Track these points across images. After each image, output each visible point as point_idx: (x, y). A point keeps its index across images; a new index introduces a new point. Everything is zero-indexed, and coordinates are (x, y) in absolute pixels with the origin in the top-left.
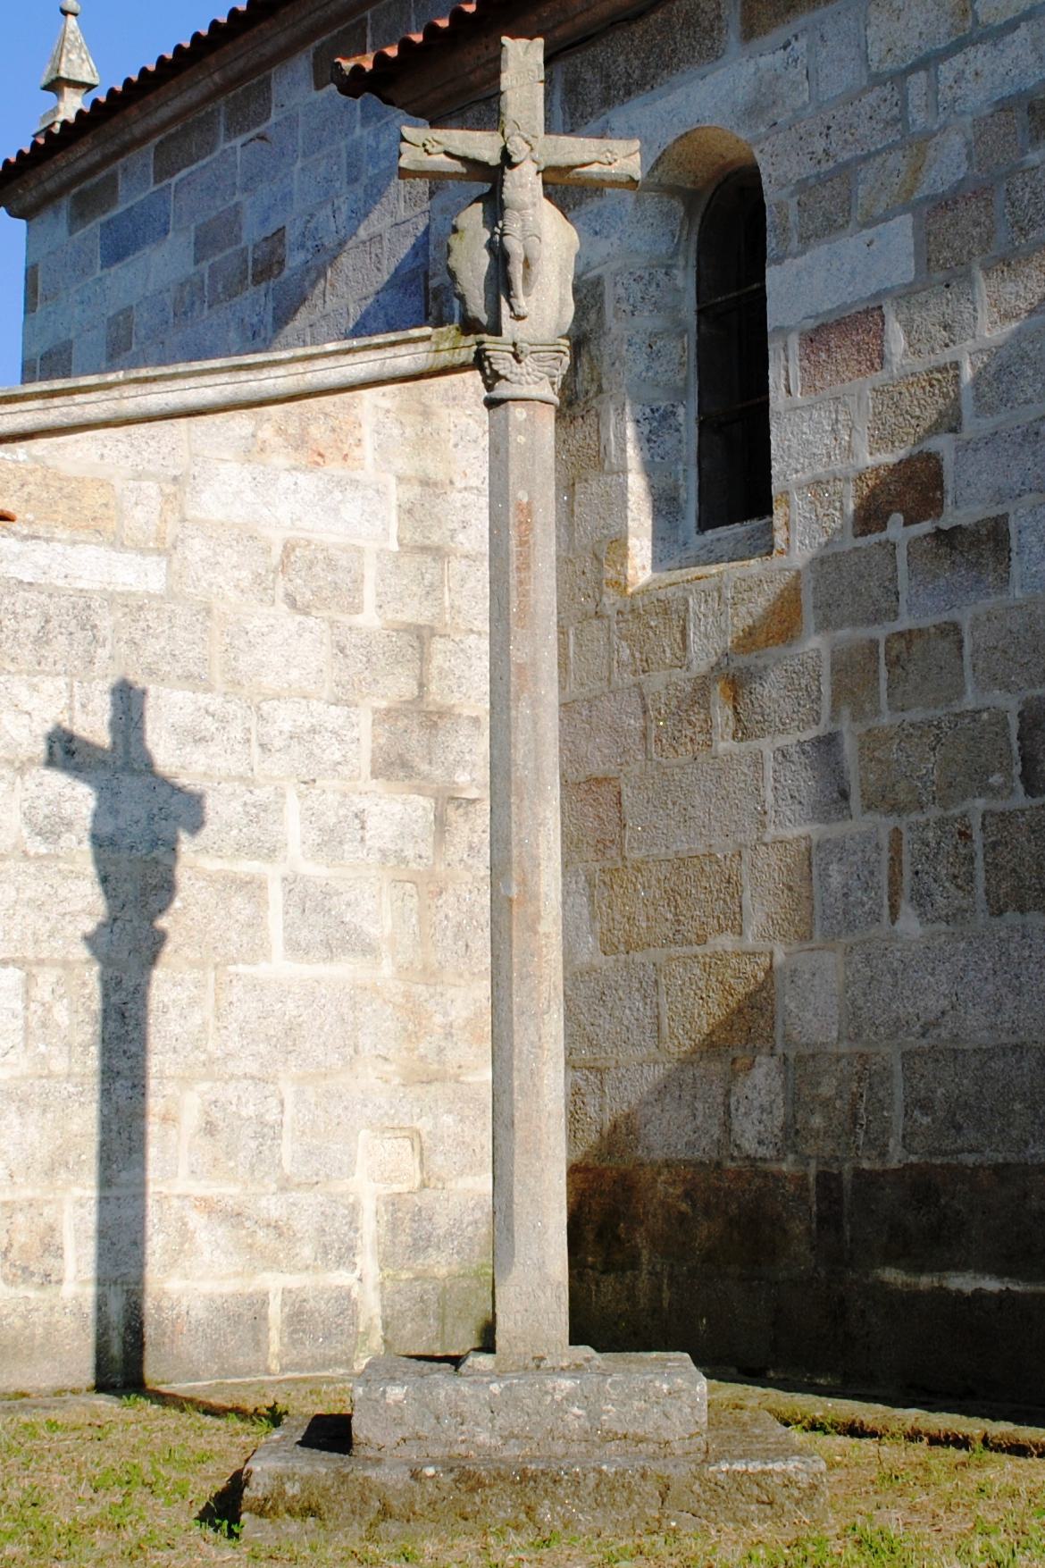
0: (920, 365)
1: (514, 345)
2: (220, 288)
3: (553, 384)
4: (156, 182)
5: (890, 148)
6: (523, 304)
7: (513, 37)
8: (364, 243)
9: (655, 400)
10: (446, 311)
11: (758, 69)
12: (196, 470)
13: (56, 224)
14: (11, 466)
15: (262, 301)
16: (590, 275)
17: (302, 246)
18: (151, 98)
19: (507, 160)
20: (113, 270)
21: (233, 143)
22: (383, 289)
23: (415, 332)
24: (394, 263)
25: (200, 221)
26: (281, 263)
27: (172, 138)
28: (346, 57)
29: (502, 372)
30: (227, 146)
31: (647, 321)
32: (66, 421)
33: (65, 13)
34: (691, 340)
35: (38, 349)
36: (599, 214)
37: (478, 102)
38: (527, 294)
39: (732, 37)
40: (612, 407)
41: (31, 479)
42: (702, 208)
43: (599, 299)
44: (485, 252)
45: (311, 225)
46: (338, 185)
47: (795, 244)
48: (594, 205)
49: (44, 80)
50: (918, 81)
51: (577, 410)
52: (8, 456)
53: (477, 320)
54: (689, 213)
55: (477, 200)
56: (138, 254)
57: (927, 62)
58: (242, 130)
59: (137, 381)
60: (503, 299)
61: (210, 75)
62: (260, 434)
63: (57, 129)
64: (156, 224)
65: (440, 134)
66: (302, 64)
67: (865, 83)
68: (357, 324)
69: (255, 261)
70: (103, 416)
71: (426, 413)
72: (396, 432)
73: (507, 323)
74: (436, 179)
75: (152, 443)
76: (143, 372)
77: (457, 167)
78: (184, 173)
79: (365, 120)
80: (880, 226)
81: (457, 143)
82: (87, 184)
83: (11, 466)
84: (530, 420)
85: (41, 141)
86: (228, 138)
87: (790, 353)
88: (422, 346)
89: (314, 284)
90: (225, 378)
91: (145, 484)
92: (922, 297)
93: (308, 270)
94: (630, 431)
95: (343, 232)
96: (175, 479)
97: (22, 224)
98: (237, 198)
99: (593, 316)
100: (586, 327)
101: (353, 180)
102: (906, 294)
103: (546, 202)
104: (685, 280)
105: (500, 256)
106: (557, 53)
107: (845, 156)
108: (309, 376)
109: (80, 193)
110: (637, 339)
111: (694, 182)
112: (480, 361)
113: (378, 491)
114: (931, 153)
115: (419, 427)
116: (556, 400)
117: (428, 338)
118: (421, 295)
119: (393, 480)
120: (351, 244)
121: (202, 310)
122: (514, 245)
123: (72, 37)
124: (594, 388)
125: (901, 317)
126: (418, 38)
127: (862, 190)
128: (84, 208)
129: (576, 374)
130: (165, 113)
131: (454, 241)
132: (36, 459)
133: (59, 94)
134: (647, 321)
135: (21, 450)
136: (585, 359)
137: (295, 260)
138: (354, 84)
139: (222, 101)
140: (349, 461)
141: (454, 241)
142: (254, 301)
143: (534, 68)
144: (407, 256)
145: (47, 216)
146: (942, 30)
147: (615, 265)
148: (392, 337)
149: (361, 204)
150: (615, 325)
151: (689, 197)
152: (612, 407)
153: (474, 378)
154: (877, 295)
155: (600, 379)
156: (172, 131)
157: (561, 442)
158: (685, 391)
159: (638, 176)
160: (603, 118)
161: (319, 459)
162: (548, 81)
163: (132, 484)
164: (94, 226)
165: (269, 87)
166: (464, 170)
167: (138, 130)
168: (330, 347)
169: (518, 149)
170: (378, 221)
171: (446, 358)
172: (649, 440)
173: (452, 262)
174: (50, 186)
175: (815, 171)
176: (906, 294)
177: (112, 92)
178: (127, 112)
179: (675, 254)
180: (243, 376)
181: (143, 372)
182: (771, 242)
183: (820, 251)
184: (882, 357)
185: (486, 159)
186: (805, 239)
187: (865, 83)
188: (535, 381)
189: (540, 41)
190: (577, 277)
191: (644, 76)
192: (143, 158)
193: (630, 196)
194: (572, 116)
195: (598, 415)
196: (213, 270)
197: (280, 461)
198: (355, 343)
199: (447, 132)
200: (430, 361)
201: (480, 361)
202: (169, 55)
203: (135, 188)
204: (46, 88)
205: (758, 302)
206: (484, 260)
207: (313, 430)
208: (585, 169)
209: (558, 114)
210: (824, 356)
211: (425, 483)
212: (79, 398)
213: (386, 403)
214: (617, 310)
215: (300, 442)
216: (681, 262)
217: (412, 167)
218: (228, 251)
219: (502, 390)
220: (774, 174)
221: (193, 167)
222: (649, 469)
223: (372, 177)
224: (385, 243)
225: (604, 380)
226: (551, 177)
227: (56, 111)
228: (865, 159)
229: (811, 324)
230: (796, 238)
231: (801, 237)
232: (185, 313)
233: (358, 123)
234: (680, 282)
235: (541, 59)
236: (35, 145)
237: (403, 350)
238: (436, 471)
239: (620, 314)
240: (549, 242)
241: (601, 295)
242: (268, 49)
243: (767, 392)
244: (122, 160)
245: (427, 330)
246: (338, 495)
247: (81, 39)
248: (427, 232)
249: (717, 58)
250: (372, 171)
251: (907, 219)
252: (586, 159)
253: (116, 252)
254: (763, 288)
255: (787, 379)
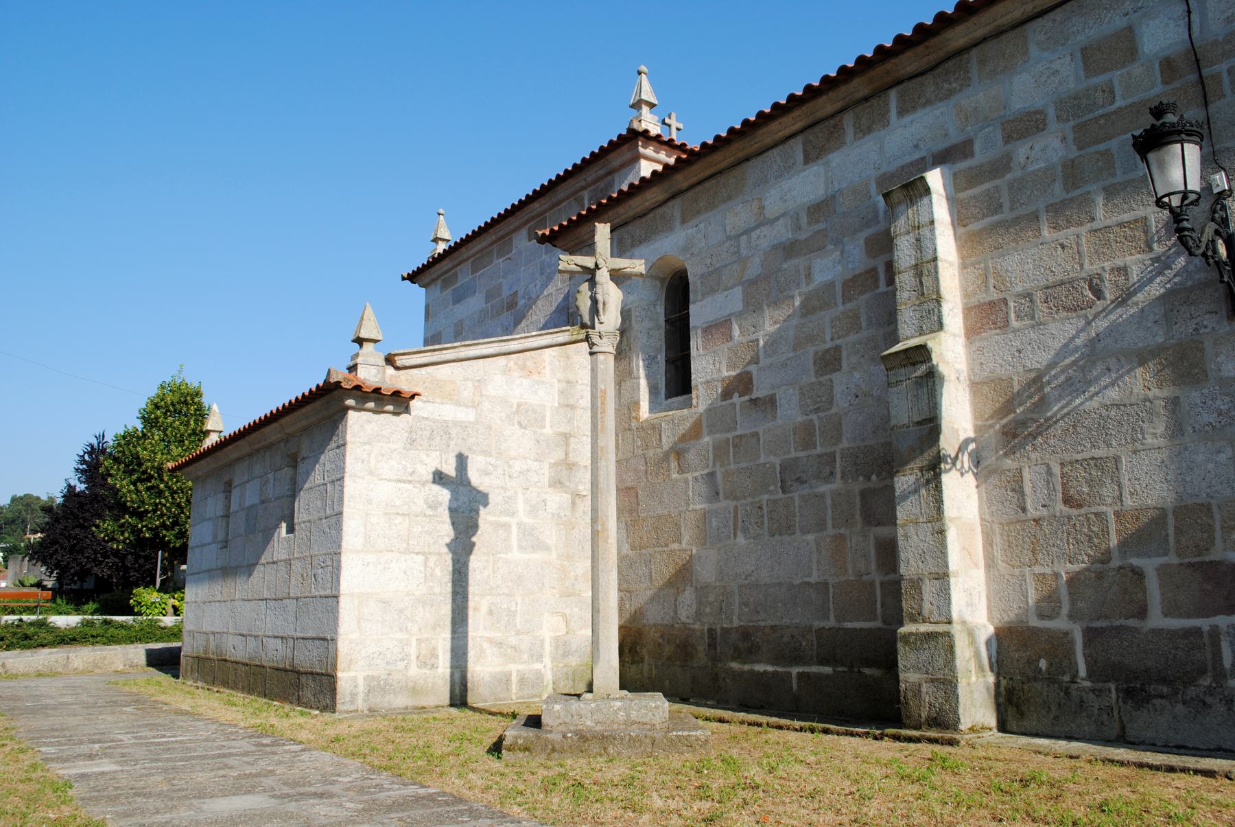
0: (744, 340)
6: (602, 318)
13: (436, 289)
31: (647, 324)
34: (662, 331)
37: (587, 246)
39: (677, 223)
47: (700, 297)
48: (628, 283)
50: (744, 239)
57: (747, 232)
65: (573, 258)
66: (524, 232)
71: (568, 357)
74: (572, 274)
77: (579, 269)
79: (547, 253)
94: (641, 363)
101: (542, 274)
102: (740, 315)
104: (661, 310)
105: (594, 301)
112: (587, 339)
118: (566, 315)
122: (599, 297)
128: (446, 285)
131: (578, 296)
134: (647, 324)
135: (423, 370)
137: (521, 302)
138: (543, 240)
141: (578, 296)
142: (507, 317)
145: (433, 287)
151: (662, 280)
153: (585, 344)
157: (616, 368)
162: (612, 239)
164: (449, 291)
167: (465, 256)
169: (601, 263)
170: (551, 289)
171: (575, 337)
172: (647, 367)
174: (434, 276)
176: (740, 315)
183: (709, 299)
186: (703, 295)
188: (607, 346)
192: (467, 266)
197: (516, 374)
201: (587, 339)
203: (464, 277)
205: (686, 318)
206: (589, 302)
211: (568, 382)
215: (523, 368)
219: (595, 349)
222: (648, 377)
240: (612, 296)
242: (512, 227)
253: (458, 299)
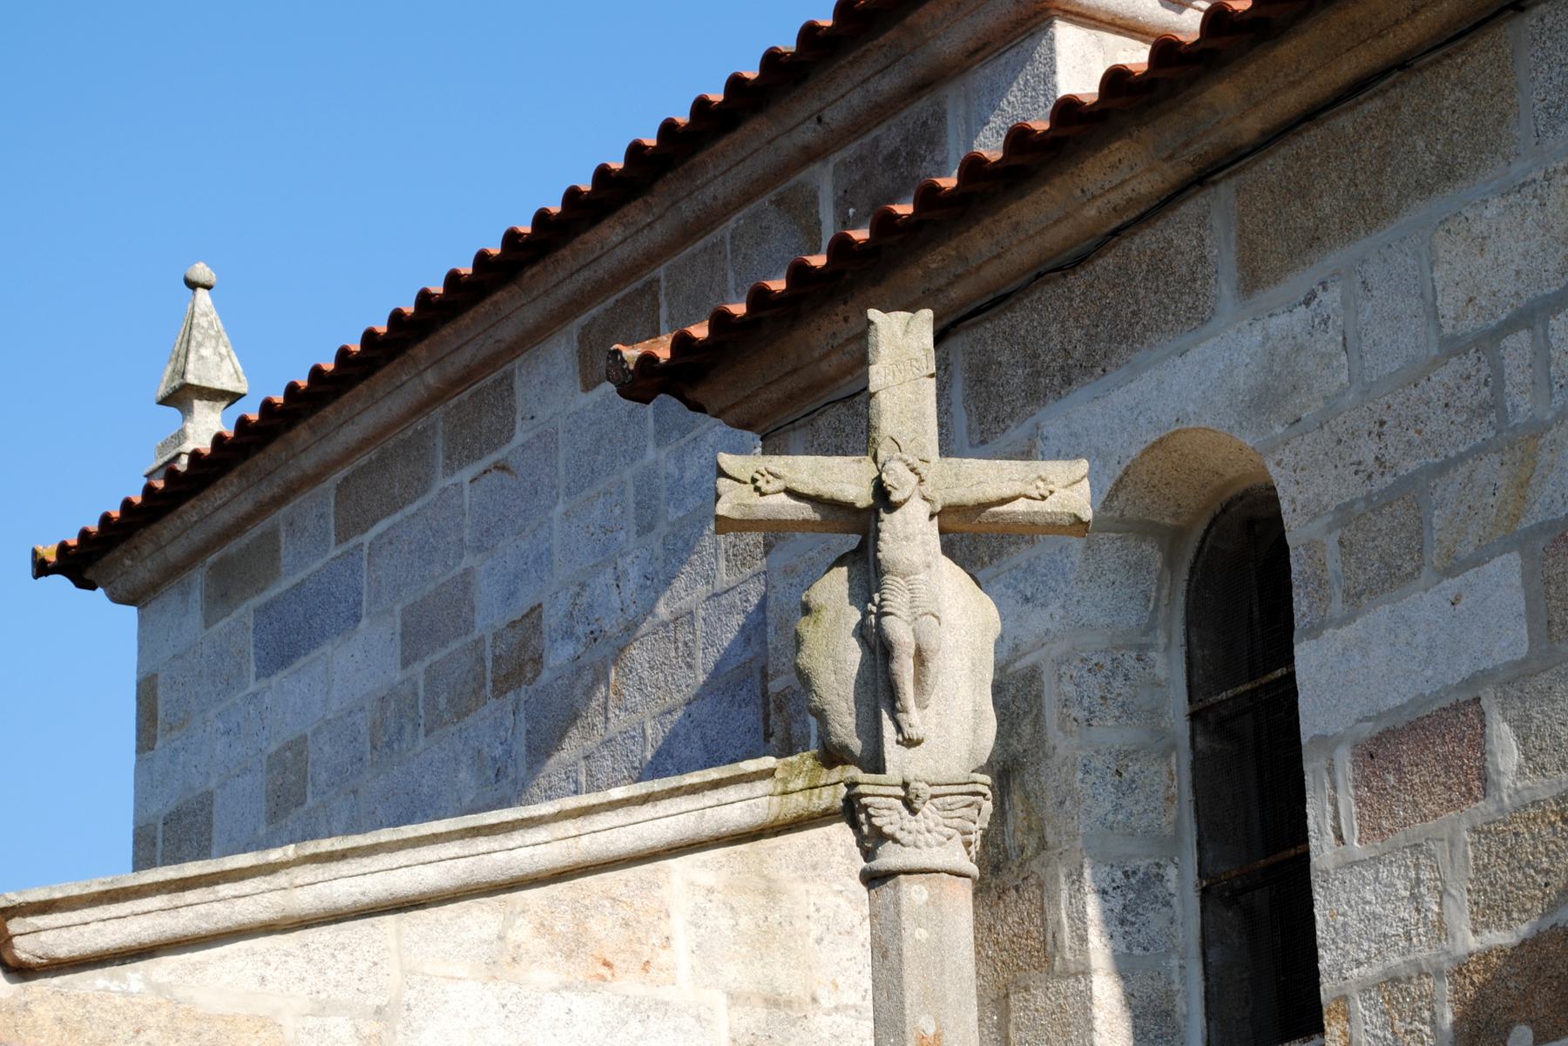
0: (1543, 788)
1: (905, 785)
2: (442, 701)
3: (968, 844)
4: (339, 542)
5: (1478, 451)
6: (915, 720)
7: (886, 310)
8: (665, 625)
9: (1131, 856)
10: (796, 729)
11: (1267, 338)
12: (410, 996)
13: (185, 612)
14: (119, 1001)
15: (509, 722)
16: (1018, 665)
17: (569, 634)
18: (328, 412)
19: (883, 498)
20: (274, 680)
21: (457, 478)
22: (697, 697)
23: (750, 766)
24: (714, 655)
25: (409, 600)
26: (538, 661)
27: (362, 472)
28: (629, 342)
29: (887, 829)
30: (449, 482)
31: (1112, 733)
32: (205, 926)
33: (193, 285)
34: (1181, 761)
35: (159, 808)
36: (1030, 569)
37: (833, 407)
38: (922, 706)
39: (1225, 289)
40: (1062, 873)
41: (151, 1020)
42: (1190, 555)
43: (1035, 702)
44: (854, 643)
45: (584, 600)
46: (622, 536)
47: (1337, 607)
48: (1020, 555)
49: (162, 391)
50: (1517, 346)
51: (1007, 878)
52: (114, 986)
53: (845, 748)
54: (1170, 563)
55: (839, 562)
56: (314, 654)
57: (1530, 317)
58: (472, 458)
59: (316, 859)
60: (885, 715)
61: (419, 374)
62: (510, 934)
63: (183, 464)
64: (341, 607)
65: (777, 463)
66: (561, 352)
67: (1435, 351)
68: (658, 754)
69: (497, 659)
70: (264, 916)
71: (771, 891)
72: (725, 922)
73: (893, 752)
74: (774, 531)
75: (341, 956)
76: (325, 845)
77: (805, 511)
78: (382, 526)
79: (662, 437)
80: (1470, 574)
81: (805, 476)
82: (233, 547)
83: (119, 1001)
84: (934, 902)
85: (160, 484)
86: (450, 470)
87: (1340, 777)
88: (762, 787)
89: (589, 693)
90: (453, 848)
91: (331, 1021)
92: (1542, 681)
93: (578, 672)
94: (1093, 908)
95: (632, 610)
96: (379, 1011)
97: (132, 611)
98: (468, 560)
99: (1026, 729)
100: (1017, 746)
101: (645, 528)
102: (1515, 679)
103: (946, 564)
104: (1169, 667)
105: (877, 648)
106: (955, 324)
107: (1411, 465)
108: (585, 839)
109: (221, 562)
110: (1097, 763)
111: (1175, 515)
112: (851, 810)
113: (698, 1018)
114: (1545, 457)
115: (760, 915)
116: (974, 870)
117: (770, 773)
118: (756, 709)
119: (722, 1000)
120: (645, 627)
121: (415, 737)
122: (899, 630)
123: (203, 322)
124: (1032, 843)
125: (1511, 713)
126: (739, 309)
127: (1438, 519)
128: (222, 596)
129: (1004, 822)
130: (351, 434)
131: (805, 626)
132: (158, 989)
133: (187, 411)
134: (1112, 733)
135: (134, 975)
136: (1016, 797)
137: (559, 656)
138: (644, 383)
139: (438, 412)
140: (653, 972)
141: (805, 626)
142: (497, 722)
143: (920, 355)
144: (734, 642)
145: (170, 599)
146: (1551, 266)
147: (1058, 649)
148: (713, 774)
149: (658, 565)
150: (1062, 742)
151: (1170, 539)
152: (1062, 873)
153: (841, 834)
154: (1472, 681)
155: (1042, 829)
156: (363, 460)
157: (984, 930)
158: (1177, 839)
159: (1087, 515)
160: (1033, 420)
161: (604, 971)
162: (943, 374)
163: (311, 1022)
164: (245, 611)
165: (511, 388)
166: (818, 517)
167: (308, 462)
168: (617, 793)
169: (900, 481)
170: (686, 592)
171: (798, 803)
172: (1121, 922)
173: (804, 660)
174: (174, 552)
175: (1362, 492)
176: (1515, 679)
177: (267, 406)
178: (292, 434)
179: (1150, 628)
180: (483, 844)
181: (325, 845)
182: (1301, 604)
183: (1379, 615)
184: (1484, 778)
185: (850, 498)
186: (1355, 598)
187: (1435, 351)
188: (939, 841)
189: (927, 314)
190: (1000, 668)
191: (1090, 354)
192: (320, 504)
193: (1077, 544)
194: (982, 419)
195: (1040, 885)
196: (432, 676)
197: (544, 975)
198: (657, 785)
199: (789, 459)
200: (775, 811)
201: (851, 810)
202: (356, 347)
203: (306, 551)
204: (165, 401)
205: (1282, 701)
206: (853, 655)
207: (594, 925)
208: (1005, 508)
209: (961, 419)
210: (1392, 779)
211: (774, 1002)
212: (225, 890)
213: (707, 878)
214: (1063, 719)
215: (574, 946)
216: (1162, 640)
217: (736, 515)
218: (455, 645)
219: (889, 857)
220: (1300, 498)
221: (397, 517)
222: (1124, 968)
223: (678, 524)
224: (699, 624)
225: (1048, 830)
226: (952, 521)
227: (181, 436)
228: (1442, 469)
229: (1368, 730)
230: (1339, 595)
231: (1346, 592)
232: (389, 744)
233: (655, 437)
234: (1161, 671)
235: (929, 340)
236: (149, 490)
237: (731, 793)
238: (790, 982)
239: (1070, 725)
240: (953, 622)
241: (1038, 696)
242: (507, 332)
243: (1305, 840)
244: (285, 509)
245: (768, 762)
246: (635, 1027)
247: (218, 325)
248: (762, 606)
249: (1203, 322)
250: (674, 514)
251: (1514, 559)
252: (1007, 492)
253: (280, 653)
254: (1291, 676)
255: (1336, 817)
